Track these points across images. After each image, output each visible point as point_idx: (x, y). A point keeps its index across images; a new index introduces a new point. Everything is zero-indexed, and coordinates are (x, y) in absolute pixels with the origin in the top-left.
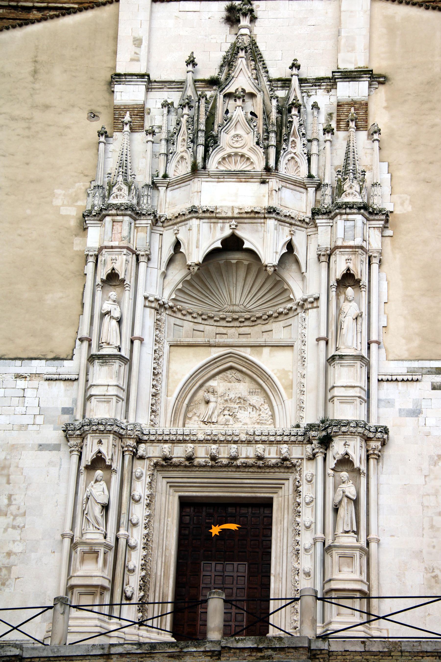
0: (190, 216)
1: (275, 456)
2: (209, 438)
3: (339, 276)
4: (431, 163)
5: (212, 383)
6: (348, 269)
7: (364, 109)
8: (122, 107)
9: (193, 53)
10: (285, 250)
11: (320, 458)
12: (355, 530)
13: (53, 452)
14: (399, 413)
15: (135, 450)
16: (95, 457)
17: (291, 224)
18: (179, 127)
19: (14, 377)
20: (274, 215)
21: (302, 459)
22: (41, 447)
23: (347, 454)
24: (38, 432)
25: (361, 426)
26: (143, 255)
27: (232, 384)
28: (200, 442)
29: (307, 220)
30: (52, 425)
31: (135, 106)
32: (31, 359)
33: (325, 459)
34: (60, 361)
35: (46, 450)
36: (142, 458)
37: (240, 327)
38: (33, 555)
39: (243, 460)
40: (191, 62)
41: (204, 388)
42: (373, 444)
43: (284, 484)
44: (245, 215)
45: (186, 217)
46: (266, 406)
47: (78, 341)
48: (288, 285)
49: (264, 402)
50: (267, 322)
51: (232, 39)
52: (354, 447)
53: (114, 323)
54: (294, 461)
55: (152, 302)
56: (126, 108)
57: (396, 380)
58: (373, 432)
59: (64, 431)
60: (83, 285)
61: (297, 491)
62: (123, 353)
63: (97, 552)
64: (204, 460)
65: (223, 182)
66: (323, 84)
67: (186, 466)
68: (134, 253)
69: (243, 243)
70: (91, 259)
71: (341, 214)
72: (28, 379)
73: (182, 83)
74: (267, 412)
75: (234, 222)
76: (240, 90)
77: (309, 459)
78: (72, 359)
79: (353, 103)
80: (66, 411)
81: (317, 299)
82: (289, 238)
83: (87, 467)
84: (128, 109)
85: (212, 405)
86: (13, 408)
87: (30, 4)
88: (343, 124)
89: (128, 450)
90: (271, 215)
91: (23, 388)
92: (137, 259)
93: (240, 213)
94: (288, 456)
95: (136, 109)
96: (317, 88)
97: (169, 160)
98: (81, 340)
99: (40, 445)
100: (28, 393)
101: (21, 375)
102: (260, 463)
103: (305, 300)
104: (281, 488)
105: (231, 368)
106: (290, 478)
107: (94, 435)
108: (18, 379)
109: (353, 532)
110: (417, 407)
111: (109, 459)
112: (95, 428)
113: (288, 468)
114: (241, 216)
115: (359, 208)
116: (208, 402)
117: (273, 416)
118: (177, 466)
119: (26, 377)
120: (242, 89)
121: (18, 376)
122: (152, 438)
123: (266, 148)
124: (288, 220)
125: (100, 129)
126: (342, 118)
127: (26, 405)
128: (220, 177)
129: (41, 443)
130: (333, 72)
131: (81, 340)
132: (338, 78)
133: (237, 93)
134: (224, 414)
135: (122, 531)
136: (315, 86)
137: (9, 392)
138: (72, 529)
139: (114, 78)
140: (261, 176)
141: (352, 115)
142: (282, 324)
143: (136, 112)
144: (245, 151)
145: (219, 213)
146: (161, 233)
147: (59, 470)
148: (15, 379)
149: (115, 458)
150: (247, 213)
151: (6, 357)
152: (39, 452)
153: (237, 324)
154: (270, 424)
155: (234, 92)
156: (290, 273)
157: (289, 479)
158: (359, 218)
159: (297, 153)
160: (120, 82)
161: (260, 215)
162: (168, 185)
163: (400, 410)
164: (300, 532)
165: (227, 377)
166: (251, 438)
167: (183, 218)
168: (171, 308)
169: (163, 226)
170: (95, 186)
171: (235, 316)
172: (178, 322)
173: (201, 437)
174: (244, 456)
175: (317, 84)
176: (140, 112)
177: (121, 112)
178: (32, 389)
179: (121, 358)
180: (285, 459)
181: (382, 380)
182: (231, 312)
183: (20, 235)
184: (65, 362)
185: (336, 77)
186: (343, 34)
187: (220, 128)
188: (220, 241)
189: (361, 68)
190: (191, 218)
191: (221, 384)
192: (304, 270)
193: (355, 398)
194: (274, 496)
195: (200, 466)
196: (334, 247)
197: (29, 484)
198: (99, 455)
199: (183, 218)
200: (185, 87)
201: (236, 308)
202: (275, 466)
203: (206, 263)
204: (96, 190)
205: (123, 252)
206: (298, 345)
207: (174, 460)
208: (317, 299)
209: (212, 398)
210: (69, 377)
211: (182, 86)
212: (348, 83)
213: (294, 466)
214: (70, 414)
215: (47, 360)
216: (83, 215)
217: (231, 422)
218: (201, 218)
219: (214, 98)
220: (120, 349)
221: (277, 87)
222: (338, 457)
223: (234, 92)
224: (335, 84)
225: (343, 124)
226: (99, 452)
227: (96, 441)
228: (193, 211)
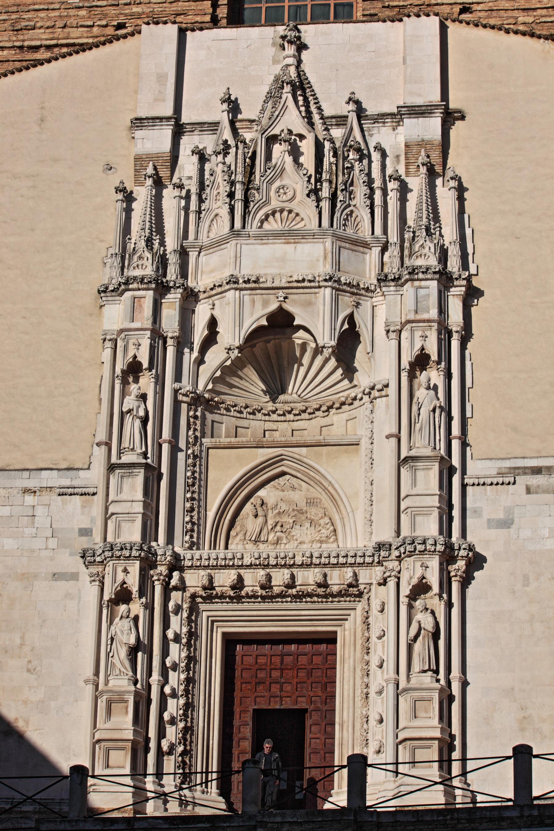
0: (227, 287)
2: (258, 562)
4: (520, 214)
5: (261, 493)
7: (437, 150)
8: (144, 157)
9: (228, 89)
10: (346, 326)
11: (392, 583)
13: (70, 582)
14: (488, 524)
15: (167, 579)
16: (119, 588)
17: (353, 294)
18: (213, 178)
19: (21, 492)
24: (52, 559)
27: (286, 493)
29: (373, 288)
30: (68, 550)
31: (160, 155)
32: (41, 469)
33: (398, 584)
34: (74, 471)
35: (62, 580)
37: (293, 421)
38: (53, 704)
43: (350, 615)
44: (295, 284)
46: (327, 520)
47: (95, 445)
49: (325, 515)
50: (326, 413)
51: (277, 70)
53: (138, 423)
56: (150, 157)
57: (484, 484)
59: (82, 557)
60: (100, 376)
63: (127, 701)
65: (267, 244)
66: (387, 120)
67: (230, 597)
69: (294, 319)
70: (108, 344)
71: (413, 280)
72: (38, 494)
73: (217, 124)
74: (328, 526)
75: (281, 293)
76: (286, 131)
77: (380, 584)
78: (88, 468)
79: (422, 144)
80: (85, 532)
81: (387, 386)
83: (110, 600)
84: (152, 159)
85: (260, 520)
86: (21, 530)
87: (38, 43)
88: (412, 168)
89: (158, 580)
91: (32, 504)
92: (165, 342)
95: (161, 159)
96: (381, 125)
97: (202, 219)
98: (98, 444)
100: (40, 511)
101: (30, 490)
104: (347, 620)
106: (357, 608)
107: (117, 562)
108: (26, 494)
110: (508, 516)
111: (136, 591)
112: (118, 553)
113: (356, 596)
114: (291, 285)
116: (256, 516)
117: (335, 531)
119: (35, 492)
120: (289, 130)
121: (26, 491)
123: (318, 200)
125: (118, 185)
126: (411, 161)
128: (263, 238)
129: (55, 571)
130: (398, 107)
131: (98, 444)
132: (404, 114)
133: (283, 135)
134: (276, 530)
135: (156, 677)
136: (378, 122)
137: (17, 510)
138: (97, 673)
139: (134, 123)
140: (314, 236)
141: (423, 159)
142: (345, 416)
143: (160, 161)
147: (79, 603)
148: (23, 495)
150: (298, 281)
151: (12, 468)
152: (54, 582)
153: (290, 417)
154: (332, 543)
155: (279, 133)
157: (355, 609)
159: (357, 206)
160: (142, 126)
162: (200, 250)
163: (489, 520)
165: (279, 484)
167: (219, 290)
170: (112, 255)
173: (247, 561)
175: (380, 121)
177: (143, 162)
178: (42, 506)
182: (283, 403)
183: (24, 318)
184: (81, 472)
185: (403, 112)
186: (408, 62)
187: (263, 179)
188: (266, 317)
189: (432, 102)
190: (229, 290)
193: (433, 509)
194: (338, 629)
196: (405, 322)
197: (44, 621)
198: (125, 586)
199: (219, 290)
200: (219, 129)
202: (340, 594)
203: (249, 344)
204: (114, 258)
205: (146, 334)
206: (365, 443)
208: (387, 386)
210: (86, 490)
211: (216, 128)
212: (417, 119)
214: (89, 536)
215: (59, 470)
216: (99, 291)
217: (285, 541)
218: (241, 289)
219: (254, 141)
221: (332, 125)
222: (415, 581)
223: (279, 133)
224: (402, 120)
225: (412, 168)
226: (125, 583)
227: (120, 569)
228: (233, 281)
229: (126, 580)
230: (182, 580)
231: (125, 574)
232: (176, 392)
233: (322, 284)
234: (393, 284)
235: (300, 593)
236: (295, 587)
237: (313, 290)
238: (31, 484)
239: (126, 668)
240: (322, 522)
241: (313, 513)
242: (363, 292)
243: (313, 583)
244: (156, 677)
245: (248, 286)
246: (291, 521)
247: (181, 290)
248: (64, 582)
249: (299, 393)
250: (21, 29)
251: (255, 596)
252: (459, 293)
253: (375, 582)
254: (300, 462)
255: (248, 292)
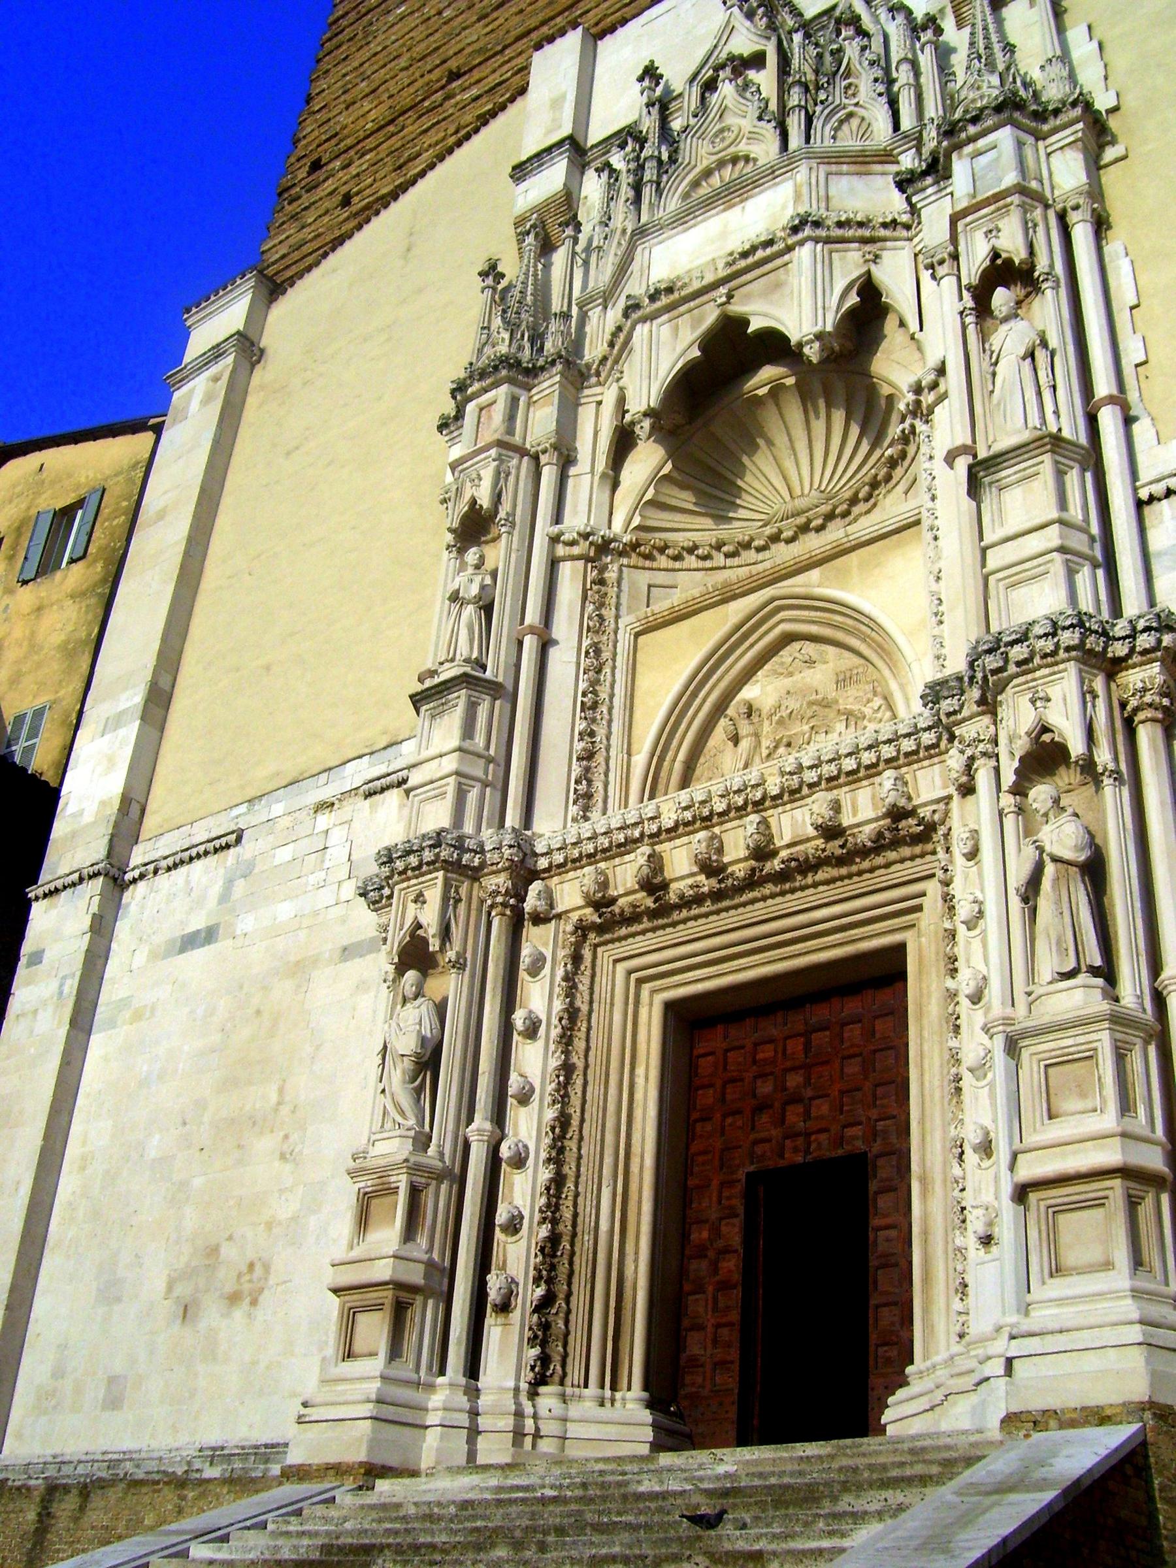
1: (871, 814)
2: (688, 815)
3: (975, 281)
5: (749, 692)
6: (996, 255)
10: (853, 299)
12: (1098, 962)
13: (368, 957)
17: (865, 241)
20: (807, 231)
21: (949, 798)
22: (348, 952)
23: (1045, 729)
25: (1068, 623)
26: (544, 452)
27: (795, 678)
28: (673, 832)
29: (905, 218)
36: (539, 919)
39: (784, 854)
40: (650, 73)
41: (731, 711)
42: (1131, 678)
43: (924, 894)
44: (743, 264)
45: (626, 329)
46: (878, 702)
48: (890, 384)
50: (872, 501)
52: (1065, 700)
54: (925, 812)
55: (572, 543)
58: (1124, 638)
61: (948, 899)
62: (488, 674)
64: (690, 881)
65: (695, 225)
68: (522, 452)
71: (959, 147)
75: (723, 290)
81: (941, 371)
82: (863, 270)
85: (745, 744)
90: (800, 236)
93: (729, 264)
94: (902, 802)
99: (345, 949)
100: (337, 836)
102: (834, 847)
103: (918, 389)
104: (919, 908)
105: (789, 638)
107: (405, 885)
109: (1094, 971)
112: (400, 865)
114: (735, 268)
115: (998, 109)
118: (632, 918)
119: (333, 804)
122: (559, 858)
124: (850, 233)
127: (326, 866)
129: (345, 943)
137: (304, 845)
140: (773, 172)
144: (743, 148)
145: (685, 285)
146: (599, 398)
149: (456, 933)
150: (745, 255)
151: (306, 775)
156: (892, 357)
158: (1005, 137)
161: (775, 248)
162: (605, 301)
164: (958, 1022)
165: (782, 664)
166: (794, 782)
168: (635, 546)
169: (599, 384)
171: (801, 520)
172: (660, 578)
174: (787, 839)
176: (561, 205)
179: (494, 689)
180: (897, 814)
181: (1152, 499)
191: (770, 688)
192: (913, 325)
193: (1048, 557)
194: (908, 936)
195: (686, 903)
201: (800, 503)
202: (879, 845)
207: (621, 902)
209: (745, 728)
213: (930, 828)
218: (651, 317)
220: (484, 668)
222: (1022, 745)
229: (424, 921)
230: (549, 897)
231: (419, 905)
232: (555, 540)
233: (790, 242)
234: (929, 180)
235: (793, 864)
236: (774, 854)
237: (778, 262)
238: (327, 793)
239: (402, 1113)
240: (867, 711)
241: (851, 700)
242: (883, 233)
243: (812, 832)
244: (481, 1123)
245: (658, 304)
246: (806, 728)
247: (559, 367)
248: (357, 960)
249: (816, 486)
250: (405, 163)
251: (699, 900)
252: (1072, 139)
253: (952, 790)
254: (809, 602)
255: (665, 317)
